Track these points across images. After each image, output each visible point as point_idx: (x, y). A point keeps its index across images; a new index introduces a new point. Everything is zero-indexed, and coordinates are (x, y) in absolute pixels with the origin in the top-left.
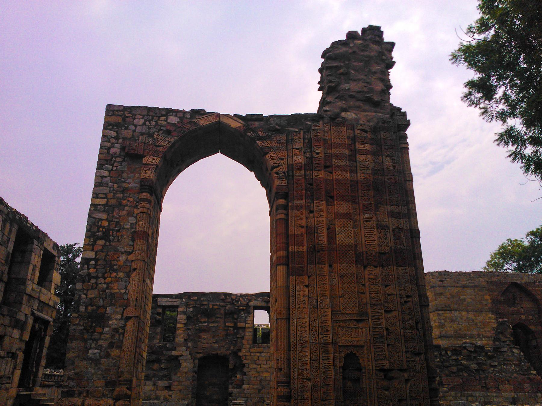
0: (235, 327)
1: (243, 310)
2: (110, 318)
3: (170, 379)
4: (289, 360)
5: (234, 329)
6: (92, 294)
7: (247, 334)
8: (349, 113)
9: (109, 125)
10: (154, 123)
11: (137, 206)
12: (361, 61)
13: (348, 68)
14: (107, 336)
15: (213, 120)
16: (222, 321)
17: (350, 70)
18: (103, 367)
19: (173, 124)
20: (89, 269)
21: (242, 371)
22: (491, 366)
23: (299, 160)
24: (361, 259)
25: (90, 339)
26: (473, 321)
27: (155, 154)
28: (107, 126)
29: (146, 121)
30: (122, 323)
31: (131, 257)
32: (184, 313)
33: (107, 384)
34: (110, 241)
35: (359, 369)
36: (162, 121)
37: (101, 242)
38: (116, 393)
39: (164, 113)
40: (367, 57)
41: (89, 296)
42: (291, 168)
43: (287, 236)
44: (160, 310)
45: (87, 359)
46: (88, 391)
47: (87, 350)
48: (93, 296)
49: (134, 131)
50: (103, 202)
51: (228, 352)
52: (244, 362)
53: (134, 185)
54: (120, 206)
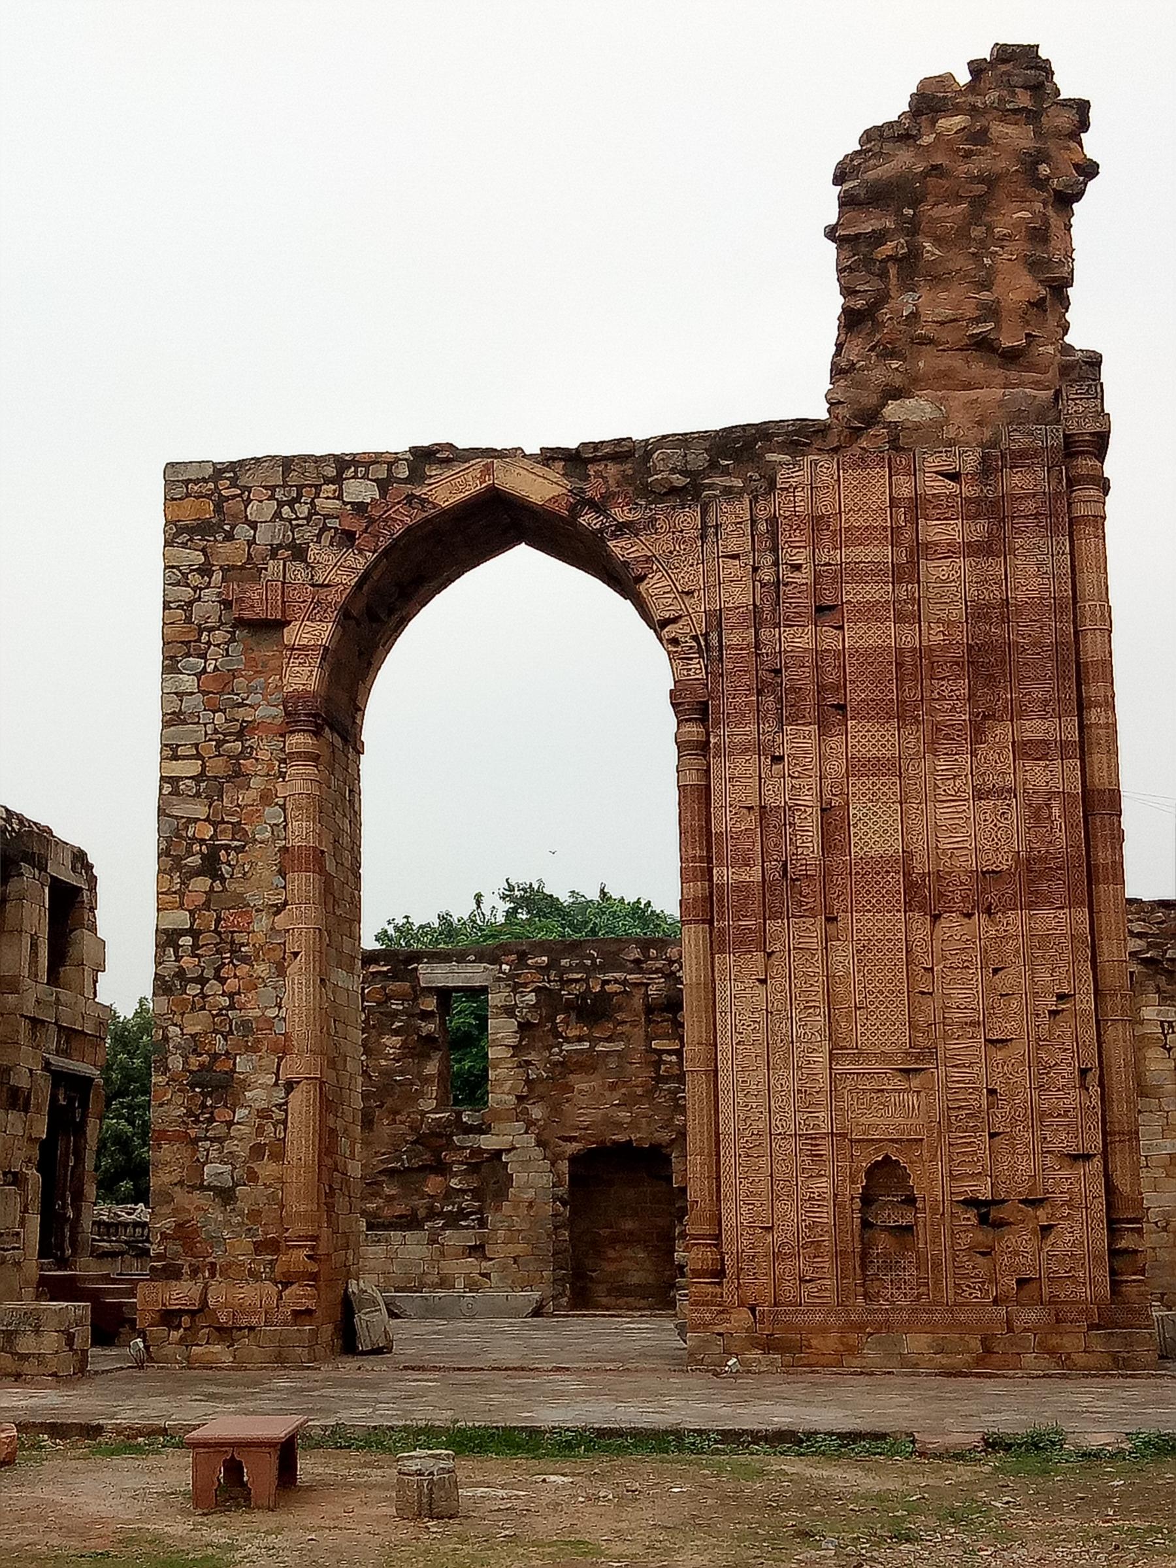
2: (245, 1085)
6: (196, 1024)
8: (910, 403)
9: (181, 530)
10: (304, 510)
11: (282, 775)
12: (959, 199)
17: (920, 238)
20: (178, 959)
23: (738, 595)
25: (206, 1139)
28: (178, 532)
29: (281, 504)
33: (259, 1248)
34: (223, 879)
36: (325, 504)
37: (201, 884)
40: (980, 179)
45: (202, 1188)
46: (213, 1264)
48: (198, 1029)
49: (251, 542)
53: (268, 712)
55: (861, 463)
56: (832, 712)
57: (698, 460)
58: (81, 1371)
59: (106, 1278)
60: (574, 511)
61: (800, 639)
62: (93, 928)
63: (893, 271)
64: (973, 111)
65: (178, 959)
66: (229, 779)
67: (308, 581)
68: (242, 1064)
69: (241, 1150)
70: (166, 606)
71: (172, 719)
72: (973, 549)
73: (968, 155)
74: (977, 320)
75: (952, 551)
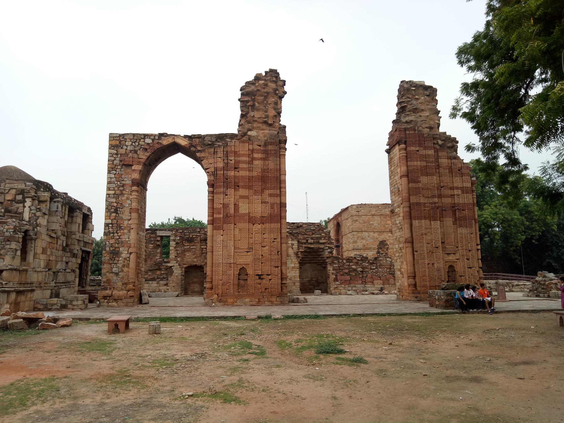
2: (122, 253)
3: (167, 280)
6: (112, 241)
9: (112, 146)
10: (137, 144)
12: (262, 96)
13: (254, 101)
15: (170, 140)
16: (199, 245)
19: (148, 144)
23: (220, 165)
24: (252, 220)
26: (377, 238)
27: (139, 163)
28: (111, 147)
30: (128, 255)
31: (130, 222)
32: (174, 240)
33: (123, 284)
35: (247, 275)
37: (114, 215)
38: (127, 288)
39: (143, 137)
40: (266, 93)
42: (216, 169)
44: (159, 239)
45: (112, 273)
47: (112, 268)
49: (126, 149)
53: (128, 182)
54: (122, 194)
55: (243, 142)
56: (237, 187)
57: (214, 139)
58: (86, 308)
59: (92, 290)
60: (190, 147)
62: (91, 223)
64: (265, 80)
66: (120, 194)
67: (136, 158)
69: (120, 266)
70: (109, 161)
71: (109, 183)
72: (261, 159)
73: (264, 88)
74: (265, 118)
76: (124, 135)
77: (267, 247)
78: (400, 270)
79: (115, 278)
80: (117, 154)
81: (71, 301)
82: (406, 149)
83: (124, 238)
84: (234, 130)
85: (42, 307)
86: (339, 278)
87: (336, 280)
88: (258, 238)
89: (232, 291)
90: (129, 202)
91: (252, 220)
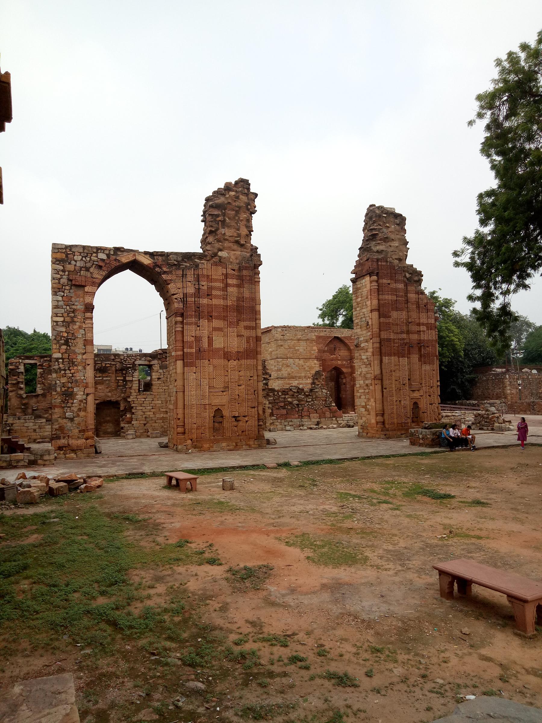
0: (124, 380)
1: (130, 367)
2: (76, 394)
4: (184, 414)
5: (123, 382)
6: (64, 380)
7: (134, 385)
8: (223, 252)
10: (88, 259)
11: (84, 322)
12: (234, 210)
13: (224, 216)
14: (76, 405)
16: (114, 376)
18: (76, 422)
20: (59, 365)
21: (131, 411)
22: (307, 401)
23: (191, 290)
24: (227, 356)
26: (303, 366)
28: (55, 261)
29: (83, 257)
30: (85, 397)
31: (84, 357)
33: (80, 431)
34: (70, 346)
35: (222, 417)
37: (64, 347)
38: (85, 436)
39: (95, 250)
41: (62, 382)
42: (185, 295)
43: (183, 341)
45: (66, 418)
46: (69, 436)
47: (65, 413)
48: (64, 381)
49: (75, 265)
50: (61, 319)
51: (119, 399)
52: (133, 405)
54: (73, 322)
57: (180, 259)
61: (204, 301)
63: (220, 223)
64: (236, 191)
65: (59, 365)
66: (71, 322)
68: (75, 390)
69: (75, 409)
73: (235, 201)
74: (237, 237)
75: (233, 286)
76: (71, 247)
77: (243, 386)
78: (365, 407)
79: (69, 424)
80: (64, 271)
81: (42, 456)
82: (377, 281)
83: (79, 376)
84: (194, 246)
85: (4, 464)
86: (275, 412)
87: (272, 414)
88: (234, 376)
89: (208, 436)
90: (82, 331)
91: (227, 356)
